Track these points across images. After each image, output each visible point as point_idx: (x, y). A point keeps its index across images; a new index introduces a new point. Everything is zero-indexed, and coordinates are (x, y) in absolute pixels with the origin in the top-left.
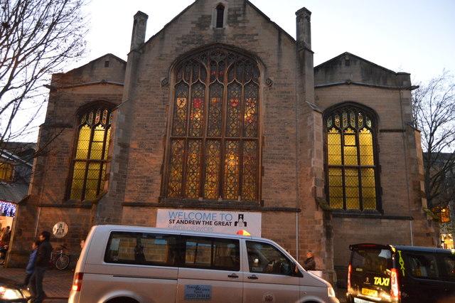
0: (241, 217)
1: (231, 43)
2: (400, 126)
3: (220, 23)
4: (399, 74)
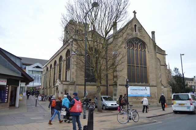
0: (146, 88)
1: (140, 38)
2: (164, 64)
3: (136, 31)
4: (163, 51)
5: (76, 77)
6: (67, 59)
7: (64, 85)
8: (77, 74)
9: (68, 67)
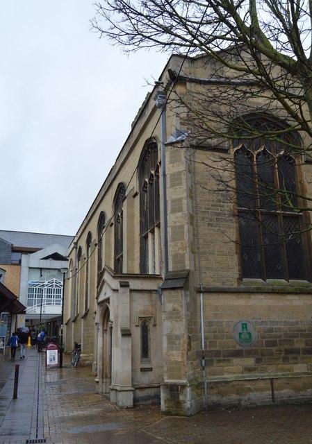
5: (193, 252)
6: (143, 187)
7: (136, 295)
8: (195, 235)
9: (150, 219)
